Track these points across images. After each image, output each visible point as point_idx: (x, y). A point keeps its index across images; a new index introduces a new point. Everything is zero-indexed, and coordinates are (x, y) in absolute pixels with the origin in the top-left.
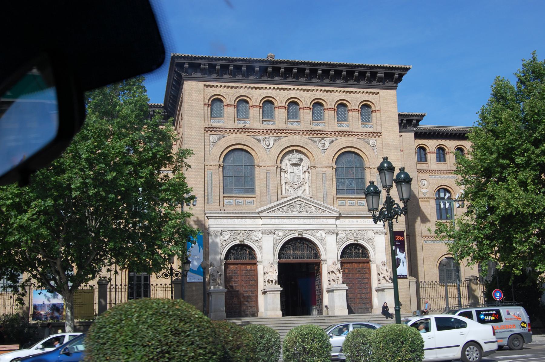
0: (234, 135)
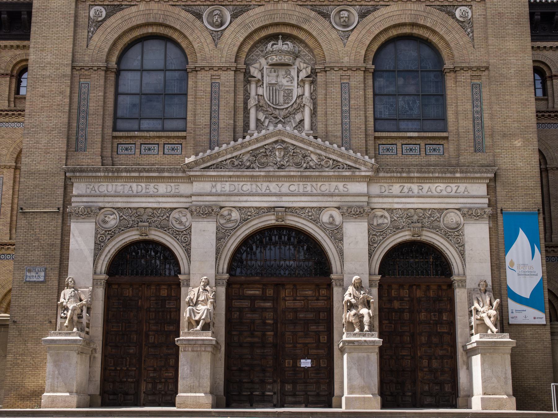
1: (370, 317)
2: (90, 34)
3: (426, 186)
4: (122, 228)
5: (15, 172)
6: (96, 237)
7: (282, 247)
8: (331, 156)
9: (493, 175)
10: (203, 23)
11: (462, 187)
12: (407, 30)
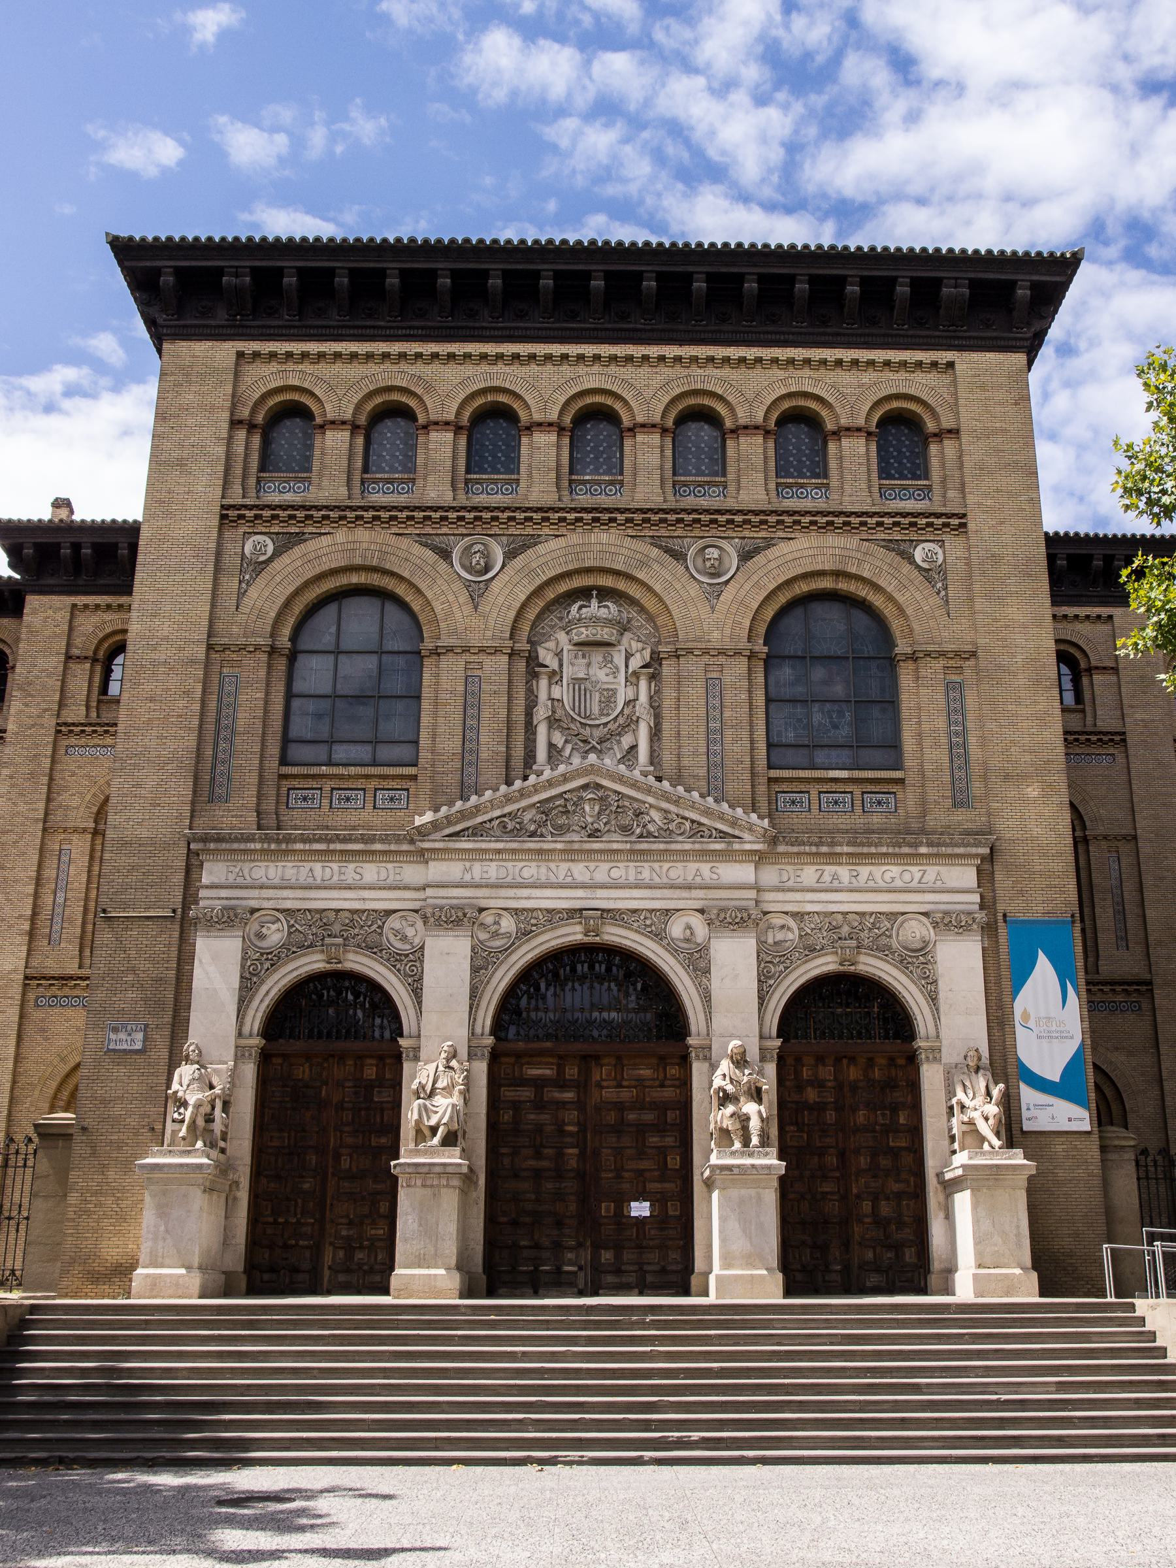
0: (341, 535)
1: (763, 1121)
2: (244, 585)
3: (864, 871)
4: (294, 947)
5: (93, 840)
6: (243, 966)
7: (596, 985)
8: (687, 814)
9: (988, 851)
10: (452, 566)
11: (932, 872)
12: (826, 584)
